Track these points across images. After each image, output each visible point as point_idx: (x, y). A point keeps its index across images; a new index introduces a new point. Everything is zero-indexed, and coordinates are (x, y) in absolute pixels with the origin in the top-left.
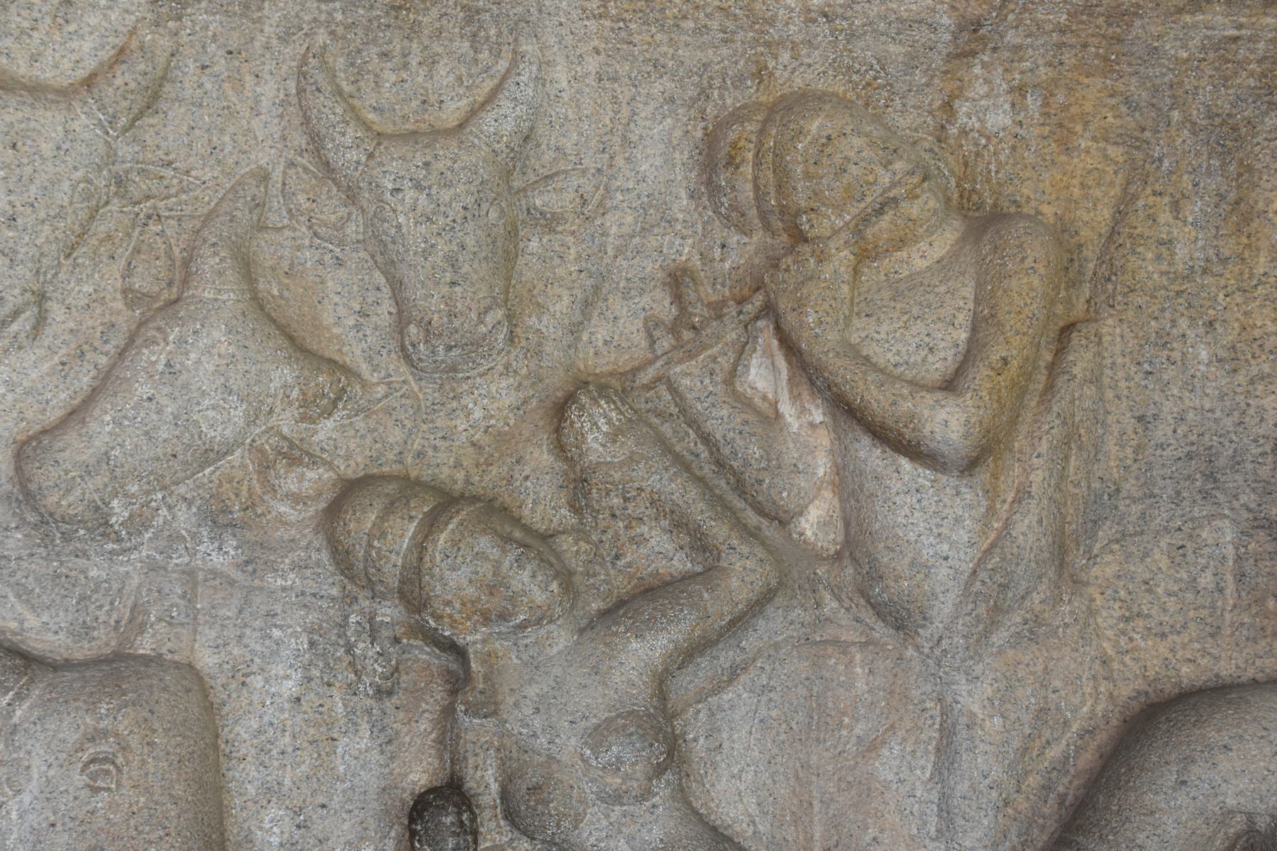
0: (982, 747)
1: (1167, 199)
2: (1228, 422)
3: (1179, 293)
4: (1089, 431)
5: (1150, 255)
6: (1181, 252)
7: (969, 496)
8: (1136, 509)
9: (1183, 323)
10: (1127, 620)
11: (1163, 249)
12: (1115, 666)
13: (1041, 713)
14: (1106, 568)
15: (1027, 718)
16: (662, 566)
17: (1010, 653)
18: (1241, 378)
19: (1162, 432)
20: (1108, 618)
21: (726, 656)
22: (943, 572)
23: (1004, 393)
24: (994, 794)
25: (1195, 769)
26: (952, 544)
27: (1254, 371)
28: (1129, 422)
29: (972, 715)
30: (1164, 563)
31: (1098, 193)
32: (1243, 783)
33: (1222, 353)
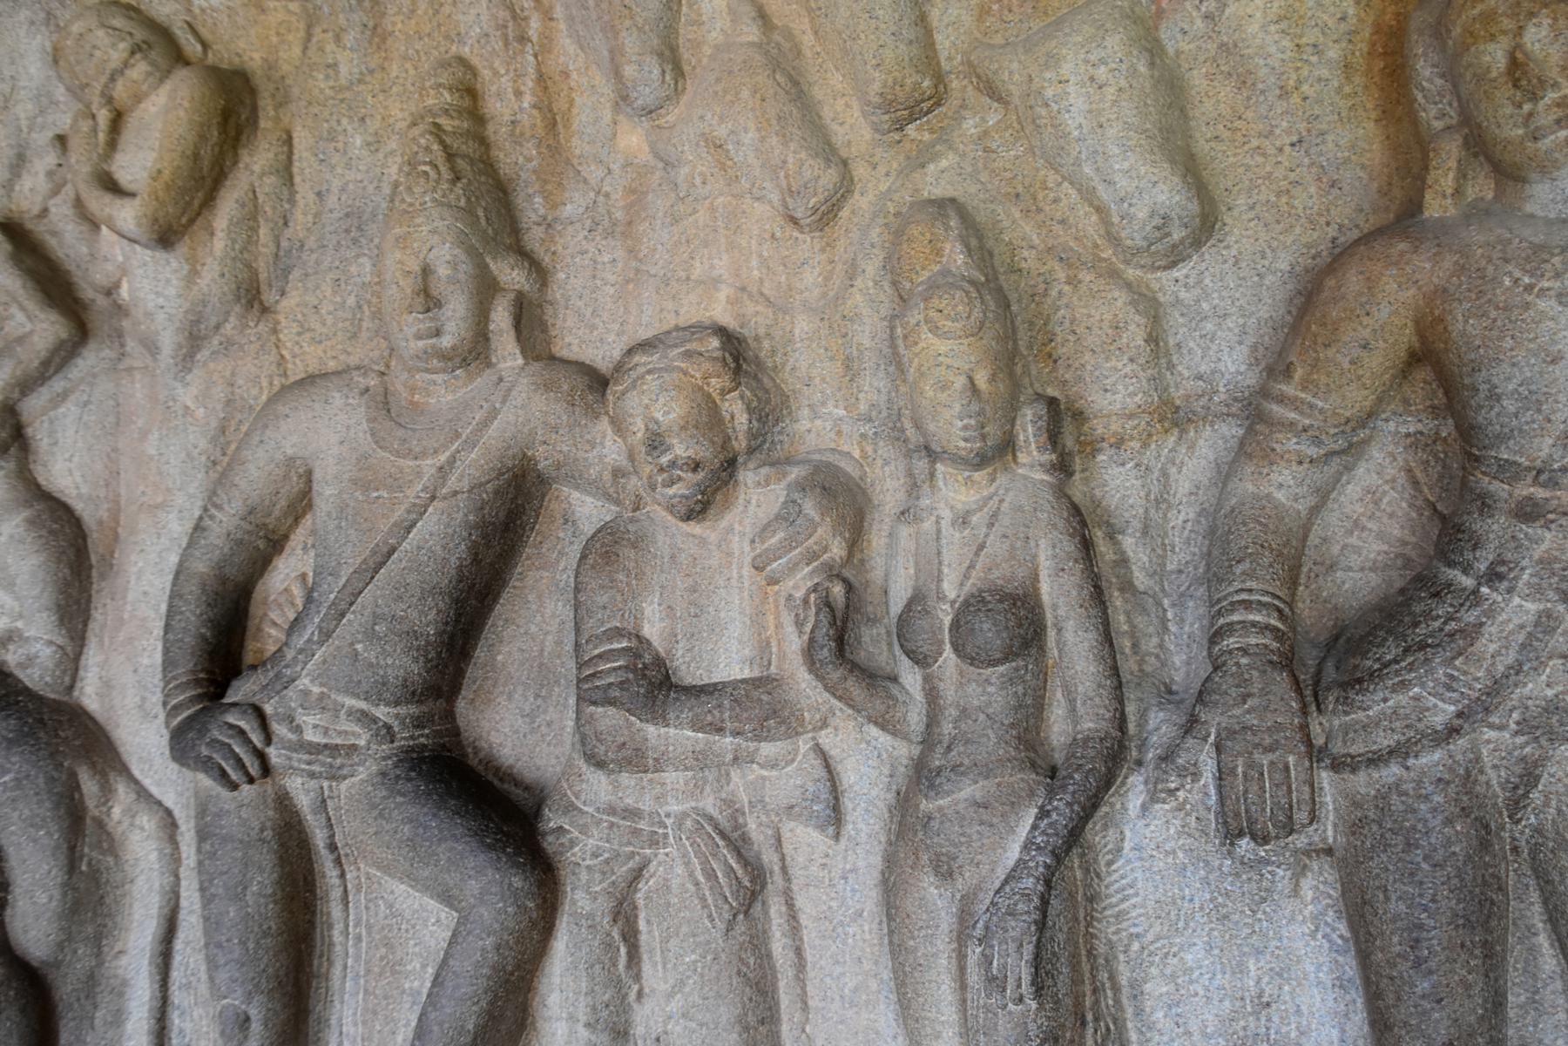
0: (191, 429)
1: (330, 34)
2: (371, 188)
3: (342, 101)
4: (274, 208)
5: (321, 76)
6: (344, 69)
7: (174, 264)
8: (314, 256)
9: (345, 121)
10: (299, 334)
11: (330, 71)
12: (290, 366)
13: (229, 402)
14: (287, 304)
15: (219, 407)
16: (21, 331)
17: (212, 365)
18: (381, 155)
19: (332, 201)
20: (288, 334)
21: (58, 384)
22: (161, 317)
23: (161, 194)
24: (203, 458)
25: (268, 432)
26: (166, 298)
27: (388, 149)
28: (311, 197)
29: (187, 408)
30: (328, 293)
31: (290, 38)
32: (295, 439)
33: (370, 139)
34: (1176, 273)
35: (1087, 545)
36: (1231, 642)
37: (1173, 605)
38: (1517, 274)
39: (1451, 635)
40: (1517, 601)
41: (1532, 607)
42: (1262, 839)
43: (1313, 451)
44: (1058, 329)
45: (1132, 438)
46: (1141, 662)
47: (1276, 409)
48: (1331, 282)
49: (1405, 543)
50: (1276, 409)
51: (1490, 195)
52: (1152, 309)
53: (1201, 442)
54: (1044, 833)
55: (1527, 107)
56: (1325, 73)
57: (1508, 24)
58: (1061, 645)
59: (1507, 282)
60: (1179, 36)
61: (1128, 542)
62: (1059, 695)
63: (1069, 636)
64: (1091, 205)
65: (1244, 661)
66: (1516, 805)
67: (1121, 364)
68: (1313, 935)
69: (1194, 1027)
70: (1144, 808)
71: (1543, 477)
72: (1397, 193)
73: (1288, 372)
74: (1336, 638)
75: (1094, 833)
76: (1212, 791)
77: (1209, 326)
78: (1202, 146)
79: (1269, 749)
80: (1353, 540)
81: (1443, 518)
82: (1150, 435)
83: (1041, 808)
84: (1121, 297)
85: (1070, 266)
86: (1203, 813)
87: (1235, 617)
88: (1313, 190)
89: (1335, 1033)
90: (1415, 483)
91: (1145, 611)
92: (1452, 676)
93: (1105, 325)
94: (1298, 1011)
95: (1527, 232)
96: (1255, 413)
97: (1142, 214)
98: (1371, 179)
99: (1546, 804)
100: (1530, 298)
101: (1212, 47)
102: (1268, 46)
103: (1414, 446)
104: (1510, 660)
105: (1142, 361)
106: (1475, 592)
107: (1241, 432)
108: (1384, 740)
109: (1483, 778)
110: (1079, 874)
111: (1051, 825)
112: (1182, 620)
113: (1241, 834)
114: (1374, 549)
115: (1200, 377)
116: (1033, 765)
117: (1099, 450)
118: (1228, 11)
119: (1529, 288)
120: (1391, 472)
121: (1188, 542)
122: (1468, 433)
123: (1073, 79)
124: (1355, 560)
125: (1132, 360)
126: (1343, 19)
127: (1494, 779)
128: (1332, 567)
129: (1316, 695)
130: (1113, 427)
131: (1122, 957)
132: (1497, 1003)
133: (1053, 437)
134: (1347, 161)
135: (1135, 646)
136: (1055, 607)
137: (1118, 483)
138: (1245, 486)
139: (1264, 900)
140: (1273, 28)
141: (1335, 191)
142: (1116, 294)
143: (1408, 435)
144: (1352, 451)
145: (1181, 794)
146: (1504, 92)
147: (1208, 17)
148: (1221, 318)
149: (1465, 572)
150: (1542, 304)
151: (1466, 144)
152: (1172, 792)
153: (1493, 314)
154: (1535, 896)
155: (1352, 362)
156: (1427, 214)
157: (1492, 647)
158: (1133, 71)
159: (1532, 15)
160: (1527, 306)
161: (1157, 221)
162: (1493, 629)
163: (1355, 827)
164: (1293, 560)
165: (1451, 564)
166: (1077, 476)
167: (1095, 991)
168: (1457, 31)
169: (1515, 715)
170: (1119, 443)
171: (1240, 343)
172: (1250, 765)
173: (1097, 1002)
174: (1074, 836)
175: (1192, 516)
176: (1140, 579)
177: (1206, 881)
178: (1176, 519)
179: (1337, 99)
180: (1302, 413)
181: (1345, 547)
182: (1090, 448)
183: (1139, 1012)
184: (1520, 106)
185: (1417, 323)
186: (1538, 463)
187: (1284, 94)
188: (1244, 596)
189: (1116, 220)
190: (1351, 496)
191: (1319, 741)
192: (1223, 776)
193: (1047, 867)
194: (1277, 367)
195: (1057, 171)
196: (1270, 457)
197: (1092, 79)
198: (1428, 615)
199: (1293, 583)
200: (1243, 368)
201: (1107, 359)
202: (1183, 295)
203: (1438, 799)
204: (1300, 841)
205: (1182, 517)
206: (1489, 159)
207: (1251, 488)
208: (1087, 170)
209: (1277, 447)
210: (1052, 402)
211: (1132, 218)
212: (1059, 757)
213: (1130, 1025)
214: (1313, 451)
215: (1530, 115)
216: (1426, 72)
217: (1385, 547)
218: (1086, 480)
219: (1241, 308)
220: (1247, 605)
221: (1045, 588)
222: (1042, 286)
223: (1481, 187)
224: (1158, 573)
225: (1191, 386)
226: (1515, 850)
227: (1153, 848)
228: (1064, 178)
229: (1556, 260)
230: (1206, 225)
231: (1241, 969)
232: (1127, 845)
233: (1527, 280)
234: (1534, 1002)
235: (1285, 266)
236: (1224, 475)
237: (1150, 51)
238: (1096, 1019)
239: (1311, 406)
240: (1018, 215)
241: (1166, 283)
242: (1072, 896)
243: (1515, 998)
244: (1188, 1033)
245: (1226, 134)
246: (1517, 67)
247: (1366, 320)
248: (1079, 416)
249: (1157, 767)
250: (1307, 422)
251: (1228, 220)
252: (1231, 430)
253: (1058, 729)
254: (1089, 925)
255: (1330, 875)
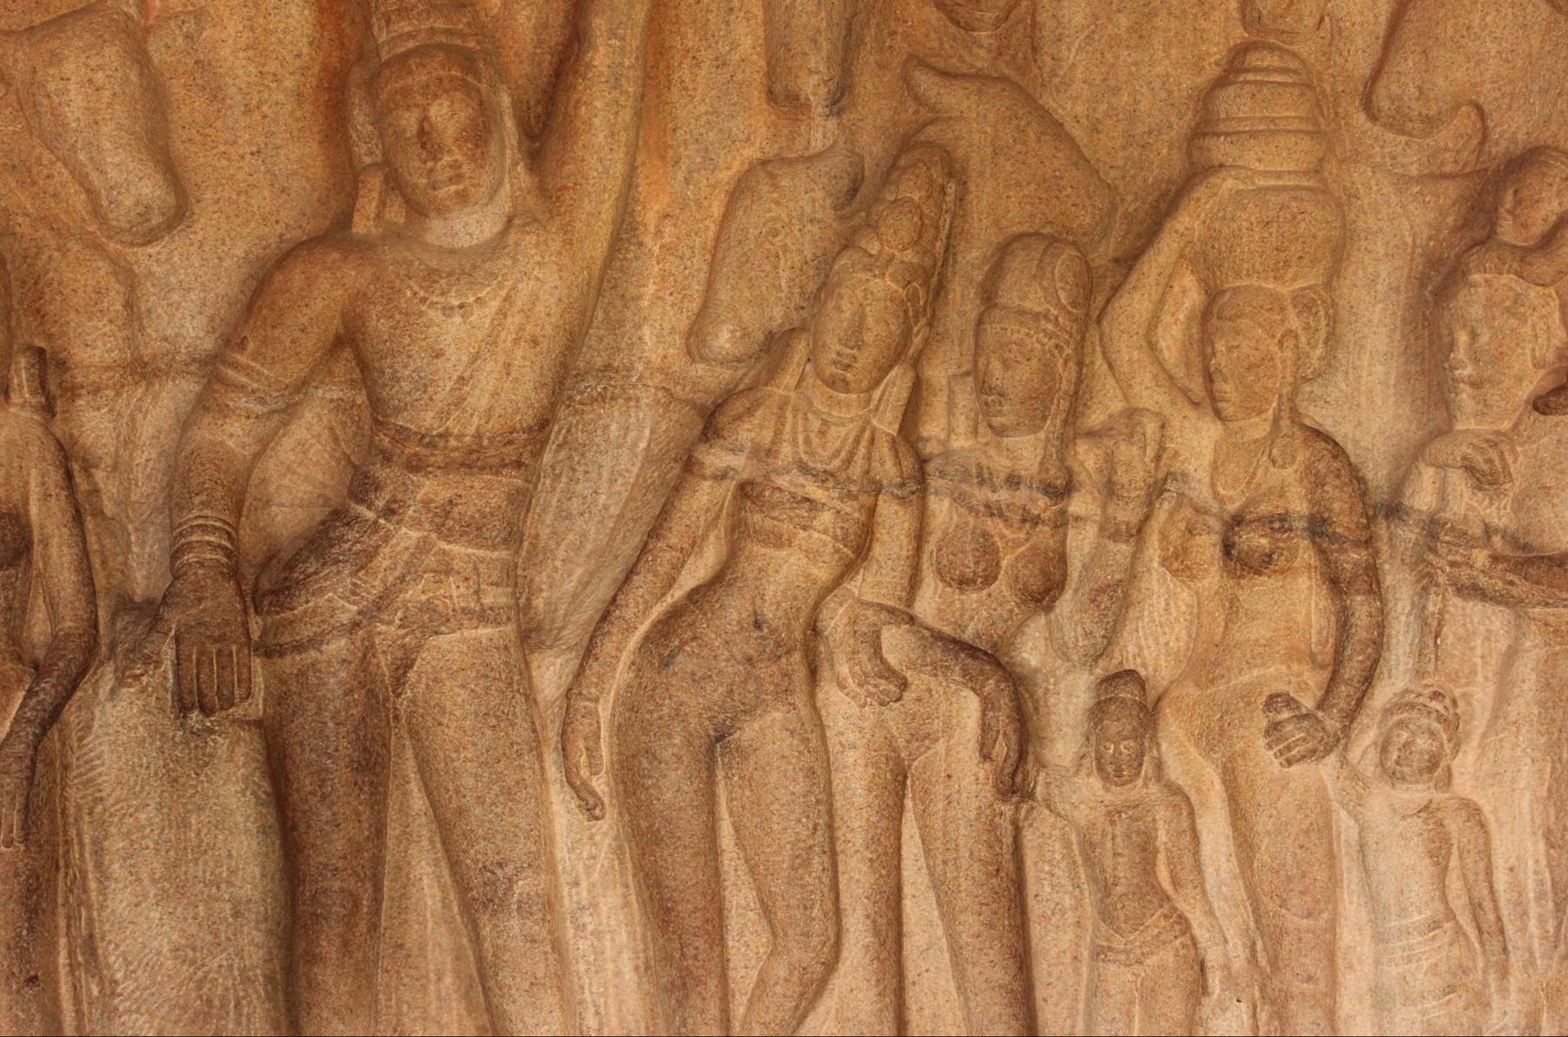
34: (150, 250)
35: (69, 476)
36: (190, 557)
37: (137, 530)
38: (416, 288)
39: (356, 554)
40: (404, 530)
41: (415, 535)
42: (207, 711)
43: (259, 409)
44: (47, 290)
45: (107, 387)
46: (109, 576)
47: (231, 373)
48: (279, 277)
49: (324, 485)
50: (231, 373)
51: (402, 221)
52: (130, 279)
53: (164, 394)
54: (33, 708)
55: (430, 164)
56: (281, 97)
57: (419, 99)
58: (46, 559)
59: (409, 294)
60: (163, 50)
61: (99, 475)
62: (40, 601)
63: (54, 551)
64: (81, 185)
65: (201, 572)
66: (399, 681)
67: (102, 324)
68: (243, 793)
69: (144, 876)
70: (113, 691)
71: (427, 440)
72: (333, 203)
73: (242, 345)
74: (269, 559)
75: (71, 715)
76: (170, 676)
77: (175, 297)
78: (179, 147)
79: (215, 641)
80: (286, 482)
81: (356, 468)
82: (123, 386)
83: (29, 691)
84: (104, 267)
85: (60, 236)
86: (162, 693)
87: (194, 538)
88: (267, 193)
89: (257, 871)
90: (336, 439)
91: (113, 534)
92: (355, 585)
93: (90, 289)
94: (230, 856)
95: (426, 256)
96: (212, 370)
97: (128, 202)
98: (314, 190)
99: (419, 681)
100: (424, 308)
101: (190, 62)
102: (237, 68)
103: (337, 409)
104: (397, 574)
105: (120, 323)
106: (375, 523)
107: (198, 388)
108: (306, 632)
109: (374, 661)
110: (58, 746)
111: (39, 702)
112: (144, 542)
113: (192, 708)
114: (303, 490)
115: (166, 339)
116: (20, 659)
117: (79, 396)
118: (205, 34)
119: (423, 300)
120: (317, 428)
121: (149, 477)
122: (375, 403)
123: (73, 78)
124: (285, 497)
125: (111, 321)
126: (298, 56)
127: (384, 663)
128: (268, 504)
129: (254, 599)
130: (92, 377)
131: (87, 818)
132: (379, 831)
133: (42, 386)
134: (294, 173)
135: (104, 562)
136: (42, 527)
137: (95, 425)
138: (206, 433)
139: (207, 764)
140: (242, 54)
141: (284, 196)
142: (100, 264)
143: (332, 401)
144: (289, 412)
145: (145, 679)
146: (415, 149)
147: (187, 36)
148: (187, 293)
149: (369, 508)
150: (431, 313)
151: (386, 180)
152: (137, 677)
153: (398, 317)
154: (409, 753)
155: (293, 342)
156: (354, 230)
157: (386, 563)
158: (126, 80)
159: (436, 96)
160: (421, 314)
161: (140, 209)
162: (387, 550)
163: (279, 698)
164: (239, 494)
165: (361, 501)
166: (58, 417)
167: (66, 842)
168: (384, 96)
169: (400, 614)
170: (96, 390)
171: (201, 313)
172: (201, 653)
173: (67, 852)
174: (53, 715)
175: (154, 456)
176: (109, 508)
177: (161, 750)
178: (140, 458)
179: (290, 121)
180: (251, 378)
181: (279, 487)
182: (72, 392)
183: (99, 865)
184: (425, 162)
185: (343, 316)
186: (423, 431)
187: (248, 111)
188: (201, 521)
189: (105, 203)
190: (286, 449)
191: (255, 636)
192: (178, 664)
193: (34, 734)
194: (231, 341)
195: (52, 152)
196: (224, 411)
197: (90, 81)
198: (341, 539)
199: (238, 509)
200: (201, 334)
201: (90, 319)
202: (155, 268)
203: (343, 674)
204: (238, 711)
205: (146, 459)
206: (403, 195)
207: (208, 436)
208: (82, 157)
209: (231, 404)
210: (41, 352)
211: (119, 204)
212: (40, 654)
213: (90, 876)
214: (259, 409)
215: (432, 170)
216: (360, 117)
217: (310, 488)
218: (65, 420)
219: (202, 284)
220: (204, 528)
221: (34, 510)
222: (34, 250)
223: (396, 213)
224: (124, 502)
225: (157, 345)
226: (396, 717)
227: (117, 726)
228: (58, 159)
229: (443, 282)
230: (179, 215)
231: (184, 824)
232: (96, 724)
233: (422, 294)
234: (406, 834)
235: (239, 252)
236: (185, 425)
237: (139, 62)
238: (67, 866)
239: (259, 373)
240: (14, 185)
241: (145, 258)
242: (52, 763)
243: (393, 831)
244: (139, 880)
245: (198, 138)
246: (425, 135)
247: (305, 310)
248: (63, 365)
249: (126, 657)
250: (255, 386)
251: (197, 211)
252: (189, 387)
253: (39, 628)
254: (63, 789)
255: (257, 744)
